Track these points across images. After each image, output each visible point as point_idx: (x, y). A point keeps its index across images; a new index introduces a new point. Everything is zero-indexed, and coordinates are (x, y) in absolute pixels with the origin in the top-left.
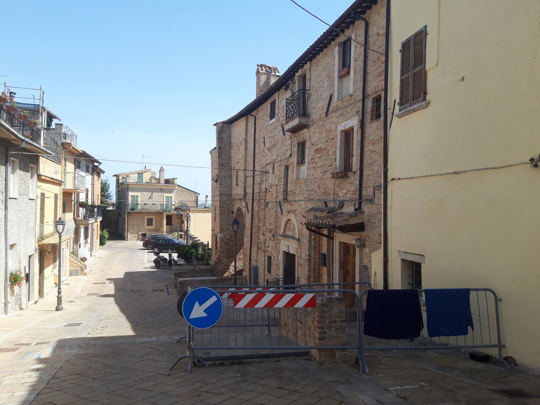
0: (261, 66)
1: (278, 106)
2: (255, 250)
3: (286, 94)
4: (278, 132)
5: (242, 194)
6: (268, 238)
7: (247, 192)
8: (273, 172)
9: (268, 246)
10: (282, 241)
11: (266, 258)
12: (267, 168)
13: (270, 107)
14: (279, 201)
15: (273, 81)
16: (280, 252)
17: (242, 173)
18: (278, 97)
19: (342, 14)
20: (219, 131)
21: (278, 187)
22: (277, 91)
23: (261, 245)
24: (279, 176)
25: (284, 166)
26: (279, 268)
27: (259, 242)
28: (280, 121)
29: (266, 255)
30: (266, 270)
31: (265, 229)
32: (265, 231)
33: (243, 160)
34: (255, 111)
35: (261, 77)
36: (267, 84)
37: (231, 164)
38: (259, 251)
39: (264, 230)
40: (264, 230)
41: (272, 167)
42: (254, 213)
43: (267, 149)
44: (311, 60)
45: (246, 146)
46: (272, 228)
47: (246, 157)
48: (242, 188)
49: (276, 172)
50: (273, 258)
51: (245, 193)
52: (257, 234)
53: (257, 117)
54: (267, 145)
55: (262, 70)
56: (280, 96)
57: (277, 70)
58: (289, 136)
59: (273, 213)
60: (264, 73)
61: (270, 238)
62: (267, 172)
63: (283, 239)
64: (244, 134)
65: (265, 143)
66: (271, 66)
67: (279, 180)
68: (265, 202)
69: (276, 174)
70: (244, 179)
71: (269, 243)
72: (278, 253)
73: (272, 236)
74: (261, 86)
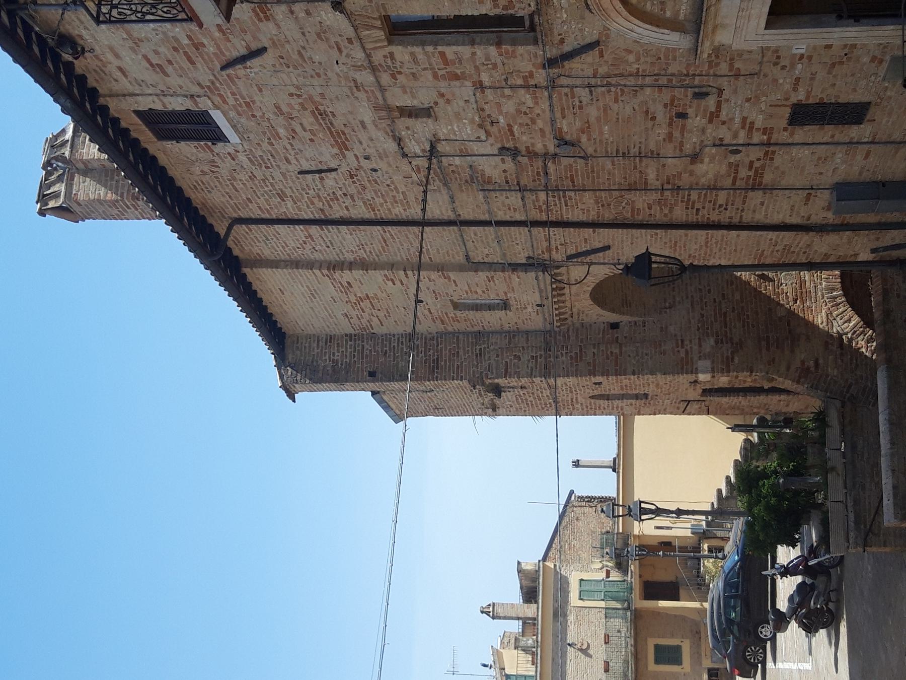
0: (43, 198)
1: (157, 95)
2: (762, 204)
3: (97, 48)
4: (260, 90)
5: (537, 278)
6: (712, 132)
7: (529, 258)
8: (426, 113)
9: (743, 128)
10: (723, 37)
11: (801, 134)
12: (418, 151)
13: (174, 142)
14: (544, 67)
15: (91, 151)
16: (773, 45)
17: (455, 281)
18: (124, 95)
19: (31, 78)
20: (310, 379)
21: (485, 78)
22: (102, 101)
23: (743, 173)
24: (435, 76)
25: (393, 48)
26: (850, 49)
27: (728, 182)
28: (213, 83)
29: (784, 137)
30: (854, 132)
31: (669, 149)
32: (681, 150)
33: (407, 276)
34: (214, 223)
35: (81, 197)
36: (106, 176)
37: (429, 336)
38: (768, 178)
39: (678, 153)
40: (678, 153)
41: (410, 122)
42: (608, 215)
43: (344, 157)
44: (93, 93)
45: (351, 266)
46: (666, 106)
47: (392, 266)
48: (514, 277)
49: (423, 98)
50: (800, 96)
51: (532, 264)
52: (694, 195)
53: (235, 215)
54: (326, 153)
55: (56, 195)
56: (116, 87)
57: (56, 137)
58: (260, 20)
59: (601, 104)
60: (66, 185)
61: (712, 113)
62: (433, 147)
63: (713, 31)
64: (308, 273)
65: (320, 167)
66: (43, 159)
67: (456, 77)
68: (555, 155)
69: (434, 96)
70: (480, 273)
71: (732, 119)
72: (776, 64)
73: (703, 102)
74: (114, 197)
